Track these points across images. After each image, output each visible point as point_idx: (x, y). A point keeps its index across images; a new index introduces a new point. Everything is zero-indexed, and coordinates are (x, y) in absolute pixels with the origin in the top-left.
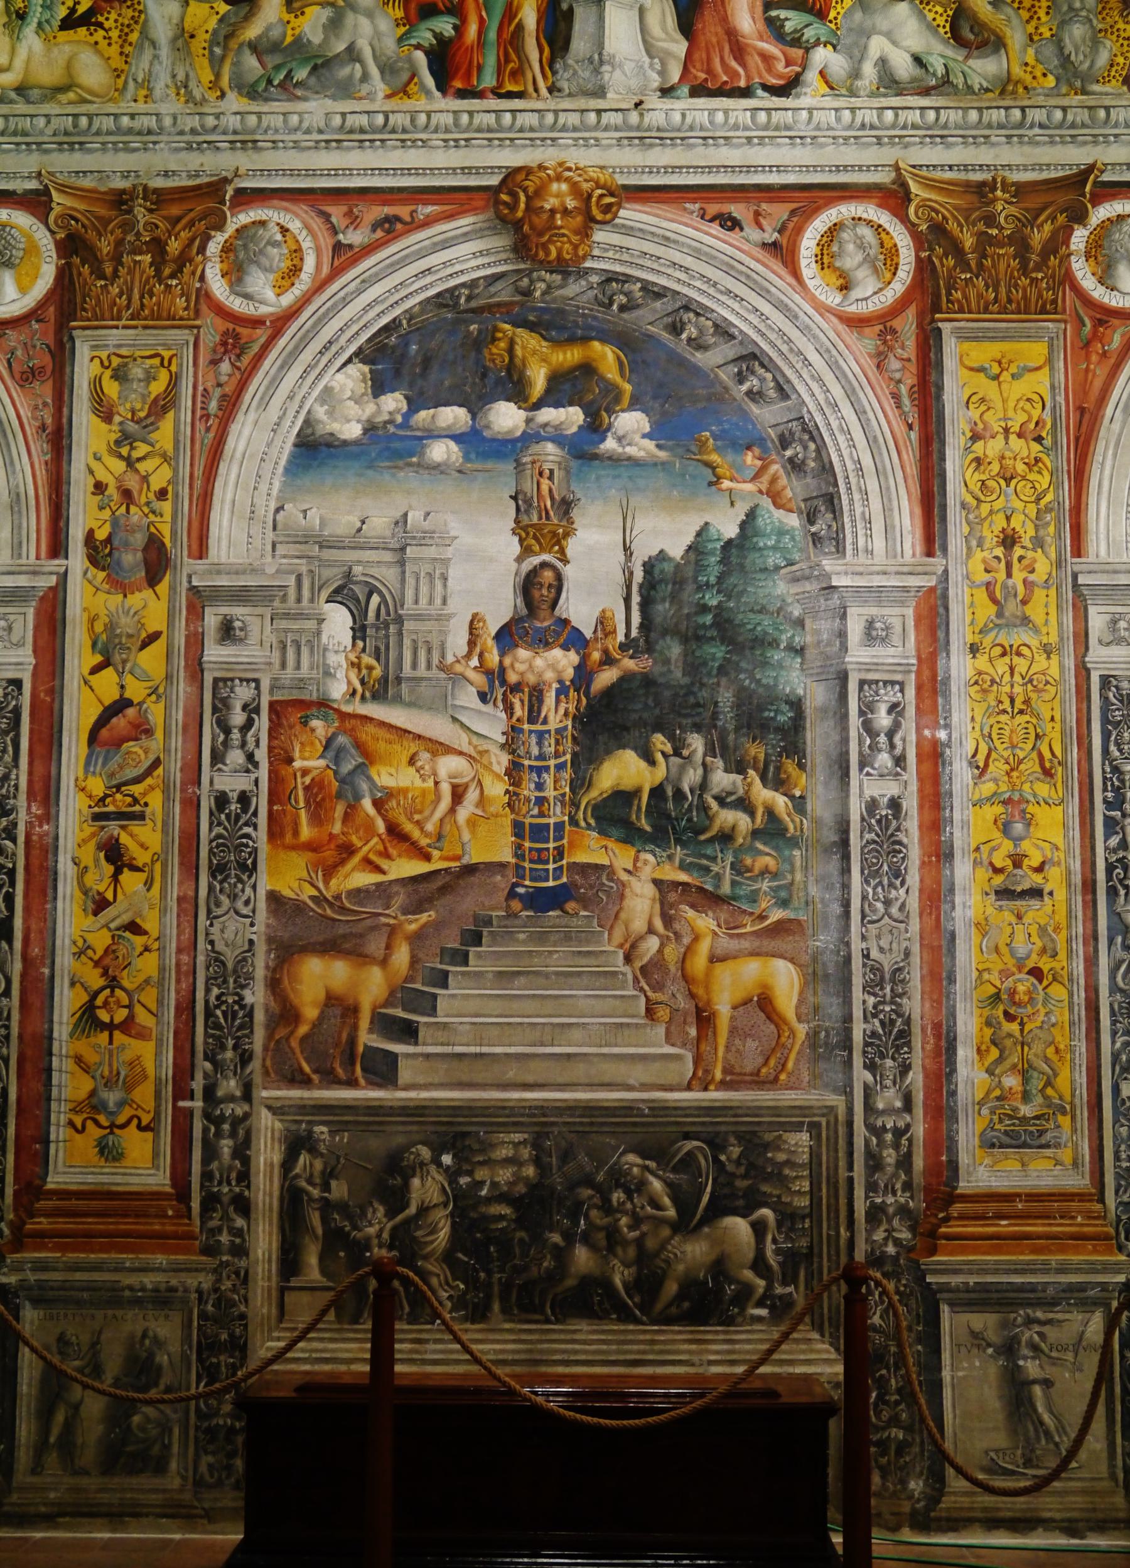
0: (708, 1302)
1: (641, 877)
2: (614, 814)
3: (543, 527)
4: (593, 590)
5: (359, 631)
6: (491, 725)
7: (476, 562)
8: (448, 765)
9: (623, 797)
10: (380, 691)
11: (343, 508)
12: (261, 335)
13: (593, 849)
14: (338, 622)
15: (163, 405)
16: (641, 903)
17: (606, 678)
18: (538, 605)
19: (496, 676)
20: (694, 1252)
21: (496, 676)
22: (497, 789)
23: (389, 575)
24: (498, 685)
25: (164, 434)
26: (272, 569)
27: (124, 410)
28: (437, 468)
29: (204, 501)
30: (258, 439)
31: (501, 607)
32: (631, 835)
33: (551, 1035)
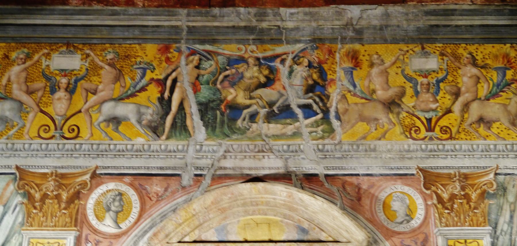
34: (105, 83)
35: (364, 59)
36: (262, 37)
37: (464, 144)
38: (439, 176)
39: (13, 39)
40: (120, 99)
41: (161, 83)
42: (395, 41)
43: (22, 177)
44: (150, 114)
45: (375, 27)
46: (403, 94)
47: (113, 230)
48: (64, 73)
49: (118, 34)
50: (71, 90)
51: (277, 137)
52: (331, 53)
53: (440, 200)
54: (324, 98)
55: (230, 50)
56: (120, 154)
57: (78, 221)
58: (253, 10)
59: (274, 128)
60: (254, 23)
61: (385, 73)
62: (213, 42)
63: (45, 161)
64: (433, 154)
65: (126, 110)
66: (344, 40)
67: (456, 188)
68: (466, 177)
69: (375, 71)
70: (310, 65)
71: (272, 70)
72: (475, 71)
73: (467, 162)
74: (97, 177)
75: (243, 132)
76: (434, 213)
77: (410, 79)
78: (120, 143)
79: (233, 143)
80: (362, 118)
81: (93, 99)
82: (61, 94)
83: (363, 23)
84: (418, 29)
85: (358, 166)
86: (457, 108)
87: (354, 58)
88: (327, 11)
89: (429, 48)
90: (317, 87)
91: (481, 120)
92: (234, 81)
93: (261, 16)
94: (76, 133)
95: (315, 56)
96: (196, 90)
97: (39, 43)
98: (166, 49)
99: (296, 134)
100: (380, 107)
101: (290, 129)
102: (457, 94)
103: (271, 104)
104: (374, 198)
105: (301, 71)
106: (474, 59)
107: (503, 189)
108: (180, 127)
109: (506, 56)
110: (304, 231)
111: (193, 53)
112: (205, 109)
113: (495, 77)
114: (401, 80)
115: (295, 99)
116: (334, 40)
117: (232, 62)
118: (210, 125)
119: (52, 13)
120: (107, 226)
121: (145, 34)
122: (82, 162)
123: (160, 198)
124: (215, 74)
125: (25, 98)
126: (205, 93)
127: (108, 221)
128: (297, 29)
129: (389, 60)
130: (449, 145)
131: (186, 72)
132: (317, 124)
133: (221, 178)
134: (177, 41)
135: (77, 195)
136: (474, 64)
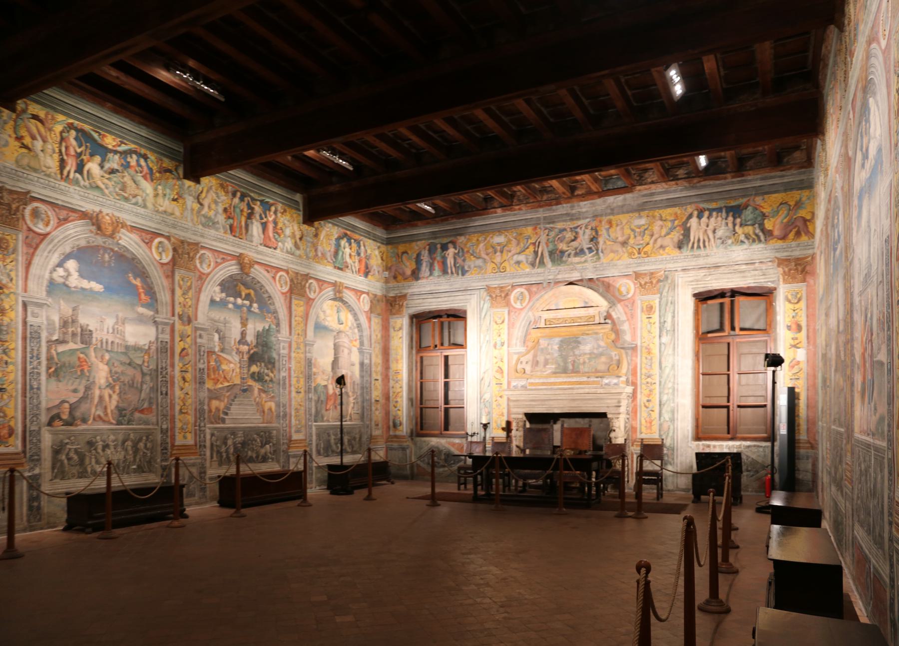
0: (264, 459)
1: (256, 386)
2: (253, 376)
3: (244, 324)
4: (250, 338)
5: (220, 339)
6: (237, 358)
7: (234, 330)
8: (232, 365)
9: (254, 373)
10: (222, 350)
11: (218, 315)
12: (204, 277)
13: (251, 382)
14: (216, 336)
15: (190, 288)
16: (256, 391)
17: (252, 352)
18: (242, 341)
19: (238, 349)
20: (263, 451)
21: (238, 349)
22: (238, 370)
23: (223, 328)
24: (239, 352)
25: (190, 294)
26: (207, 325)
27: (184, 287)
28: (230, 309)
29: (196, 309)
30: (204, 298)
31: (238, 337)
32: (255, 381)
33: (244, 415)
34: (514, 249)
35: (614, 223)
36: (573, 217)
37: (652, 259)
38: (641, 274)
39: (479, 232)
40: (519, 253)
41: (534, 244)
42: (628, 212)
43: (488, 289)
44: (531, 258)
45: (619, 206)
46: (629, 238)
47: (520, 307)
48: (499, 244)
49: (517, 224)
50: (502, 252)
51: (578, 263)
52: (600, 222)
53: (641, 285)
54: (597, 244)
55: (560, 225)
56: (521, 276)
57: (508, 304)
58: (569, 205)
59: (577, 259)
60: (570, 211)
61: (622, 229)
62: (553, 222)
63: (495, 283)
64: (639, 265)
65: (521, 257)
66: (606, 215)
67: (647, 279)
68: (652, 274)
69: (618, 228)
70: (592, 229)
71: (577, 233)
72: (660, 223)
73: (653, 267)
74: (514, 287)
75: (565, 262)
76: (638, 291)
77: (633, 230)
78: (520, 271)
79: (561, 268)
80: (613, 251)
81: (510, 254)
82: (498, 254)
83: (615, 205)
84: (639, 205)
85: (609, 273)
86: (652, 242)
87: (610, 223)
88: (599, 201)
89: (642, 213)
90: (593, 239)
91: (662, 247)
92: (561, 240)
93: (572, 207)
94: (505, 269)
95: (594, 224)
96: (547, 246)
97: (488, 232)
98: (535, 229)
99: (586, 261)
100: (619, 245)
101: (583, 259)
102: (652, 235)
103: (576, 249)
104: (614, 287)
105: (588, 232)
106: (661, 217)
107: (667, 278)
108: (542, 263)
109: (676, 214)
110: (586, 303)
111: (546, 229)
112: (551, 253)
113: (669, 224)
114: (629, 231)
115: (585, 246)
116: (601, 215)
117: (562, 230)
118: (553, 261)
119: (492, 218)
120: (518, 305)
121: (526, 223)
122: (507, 281)
123: (536, 293)
124: (554, 238)
125: (486, 257)
126: (551, 247)
127: (518, 303)
128: (587, 212)
129: (624, 222)
130: (646, 260)
131: (543, 239)
132: (593, 256)
133: (557, 283)
134: (539, 224)
135: (507, 295)
136: (661, 220)
